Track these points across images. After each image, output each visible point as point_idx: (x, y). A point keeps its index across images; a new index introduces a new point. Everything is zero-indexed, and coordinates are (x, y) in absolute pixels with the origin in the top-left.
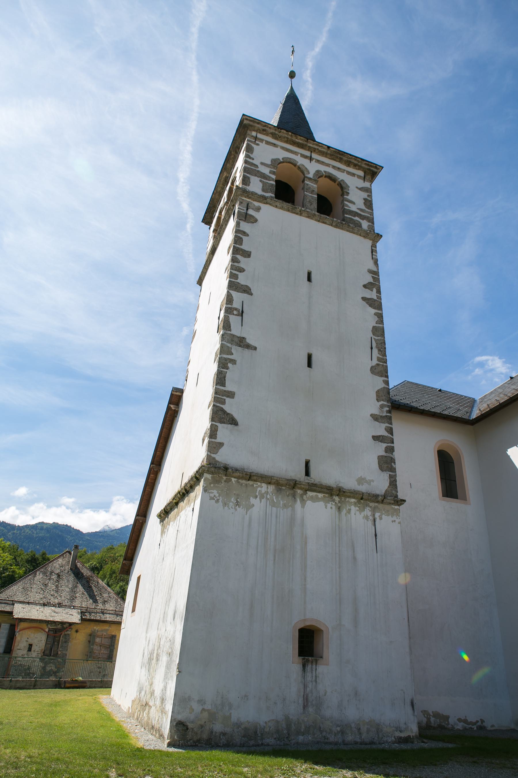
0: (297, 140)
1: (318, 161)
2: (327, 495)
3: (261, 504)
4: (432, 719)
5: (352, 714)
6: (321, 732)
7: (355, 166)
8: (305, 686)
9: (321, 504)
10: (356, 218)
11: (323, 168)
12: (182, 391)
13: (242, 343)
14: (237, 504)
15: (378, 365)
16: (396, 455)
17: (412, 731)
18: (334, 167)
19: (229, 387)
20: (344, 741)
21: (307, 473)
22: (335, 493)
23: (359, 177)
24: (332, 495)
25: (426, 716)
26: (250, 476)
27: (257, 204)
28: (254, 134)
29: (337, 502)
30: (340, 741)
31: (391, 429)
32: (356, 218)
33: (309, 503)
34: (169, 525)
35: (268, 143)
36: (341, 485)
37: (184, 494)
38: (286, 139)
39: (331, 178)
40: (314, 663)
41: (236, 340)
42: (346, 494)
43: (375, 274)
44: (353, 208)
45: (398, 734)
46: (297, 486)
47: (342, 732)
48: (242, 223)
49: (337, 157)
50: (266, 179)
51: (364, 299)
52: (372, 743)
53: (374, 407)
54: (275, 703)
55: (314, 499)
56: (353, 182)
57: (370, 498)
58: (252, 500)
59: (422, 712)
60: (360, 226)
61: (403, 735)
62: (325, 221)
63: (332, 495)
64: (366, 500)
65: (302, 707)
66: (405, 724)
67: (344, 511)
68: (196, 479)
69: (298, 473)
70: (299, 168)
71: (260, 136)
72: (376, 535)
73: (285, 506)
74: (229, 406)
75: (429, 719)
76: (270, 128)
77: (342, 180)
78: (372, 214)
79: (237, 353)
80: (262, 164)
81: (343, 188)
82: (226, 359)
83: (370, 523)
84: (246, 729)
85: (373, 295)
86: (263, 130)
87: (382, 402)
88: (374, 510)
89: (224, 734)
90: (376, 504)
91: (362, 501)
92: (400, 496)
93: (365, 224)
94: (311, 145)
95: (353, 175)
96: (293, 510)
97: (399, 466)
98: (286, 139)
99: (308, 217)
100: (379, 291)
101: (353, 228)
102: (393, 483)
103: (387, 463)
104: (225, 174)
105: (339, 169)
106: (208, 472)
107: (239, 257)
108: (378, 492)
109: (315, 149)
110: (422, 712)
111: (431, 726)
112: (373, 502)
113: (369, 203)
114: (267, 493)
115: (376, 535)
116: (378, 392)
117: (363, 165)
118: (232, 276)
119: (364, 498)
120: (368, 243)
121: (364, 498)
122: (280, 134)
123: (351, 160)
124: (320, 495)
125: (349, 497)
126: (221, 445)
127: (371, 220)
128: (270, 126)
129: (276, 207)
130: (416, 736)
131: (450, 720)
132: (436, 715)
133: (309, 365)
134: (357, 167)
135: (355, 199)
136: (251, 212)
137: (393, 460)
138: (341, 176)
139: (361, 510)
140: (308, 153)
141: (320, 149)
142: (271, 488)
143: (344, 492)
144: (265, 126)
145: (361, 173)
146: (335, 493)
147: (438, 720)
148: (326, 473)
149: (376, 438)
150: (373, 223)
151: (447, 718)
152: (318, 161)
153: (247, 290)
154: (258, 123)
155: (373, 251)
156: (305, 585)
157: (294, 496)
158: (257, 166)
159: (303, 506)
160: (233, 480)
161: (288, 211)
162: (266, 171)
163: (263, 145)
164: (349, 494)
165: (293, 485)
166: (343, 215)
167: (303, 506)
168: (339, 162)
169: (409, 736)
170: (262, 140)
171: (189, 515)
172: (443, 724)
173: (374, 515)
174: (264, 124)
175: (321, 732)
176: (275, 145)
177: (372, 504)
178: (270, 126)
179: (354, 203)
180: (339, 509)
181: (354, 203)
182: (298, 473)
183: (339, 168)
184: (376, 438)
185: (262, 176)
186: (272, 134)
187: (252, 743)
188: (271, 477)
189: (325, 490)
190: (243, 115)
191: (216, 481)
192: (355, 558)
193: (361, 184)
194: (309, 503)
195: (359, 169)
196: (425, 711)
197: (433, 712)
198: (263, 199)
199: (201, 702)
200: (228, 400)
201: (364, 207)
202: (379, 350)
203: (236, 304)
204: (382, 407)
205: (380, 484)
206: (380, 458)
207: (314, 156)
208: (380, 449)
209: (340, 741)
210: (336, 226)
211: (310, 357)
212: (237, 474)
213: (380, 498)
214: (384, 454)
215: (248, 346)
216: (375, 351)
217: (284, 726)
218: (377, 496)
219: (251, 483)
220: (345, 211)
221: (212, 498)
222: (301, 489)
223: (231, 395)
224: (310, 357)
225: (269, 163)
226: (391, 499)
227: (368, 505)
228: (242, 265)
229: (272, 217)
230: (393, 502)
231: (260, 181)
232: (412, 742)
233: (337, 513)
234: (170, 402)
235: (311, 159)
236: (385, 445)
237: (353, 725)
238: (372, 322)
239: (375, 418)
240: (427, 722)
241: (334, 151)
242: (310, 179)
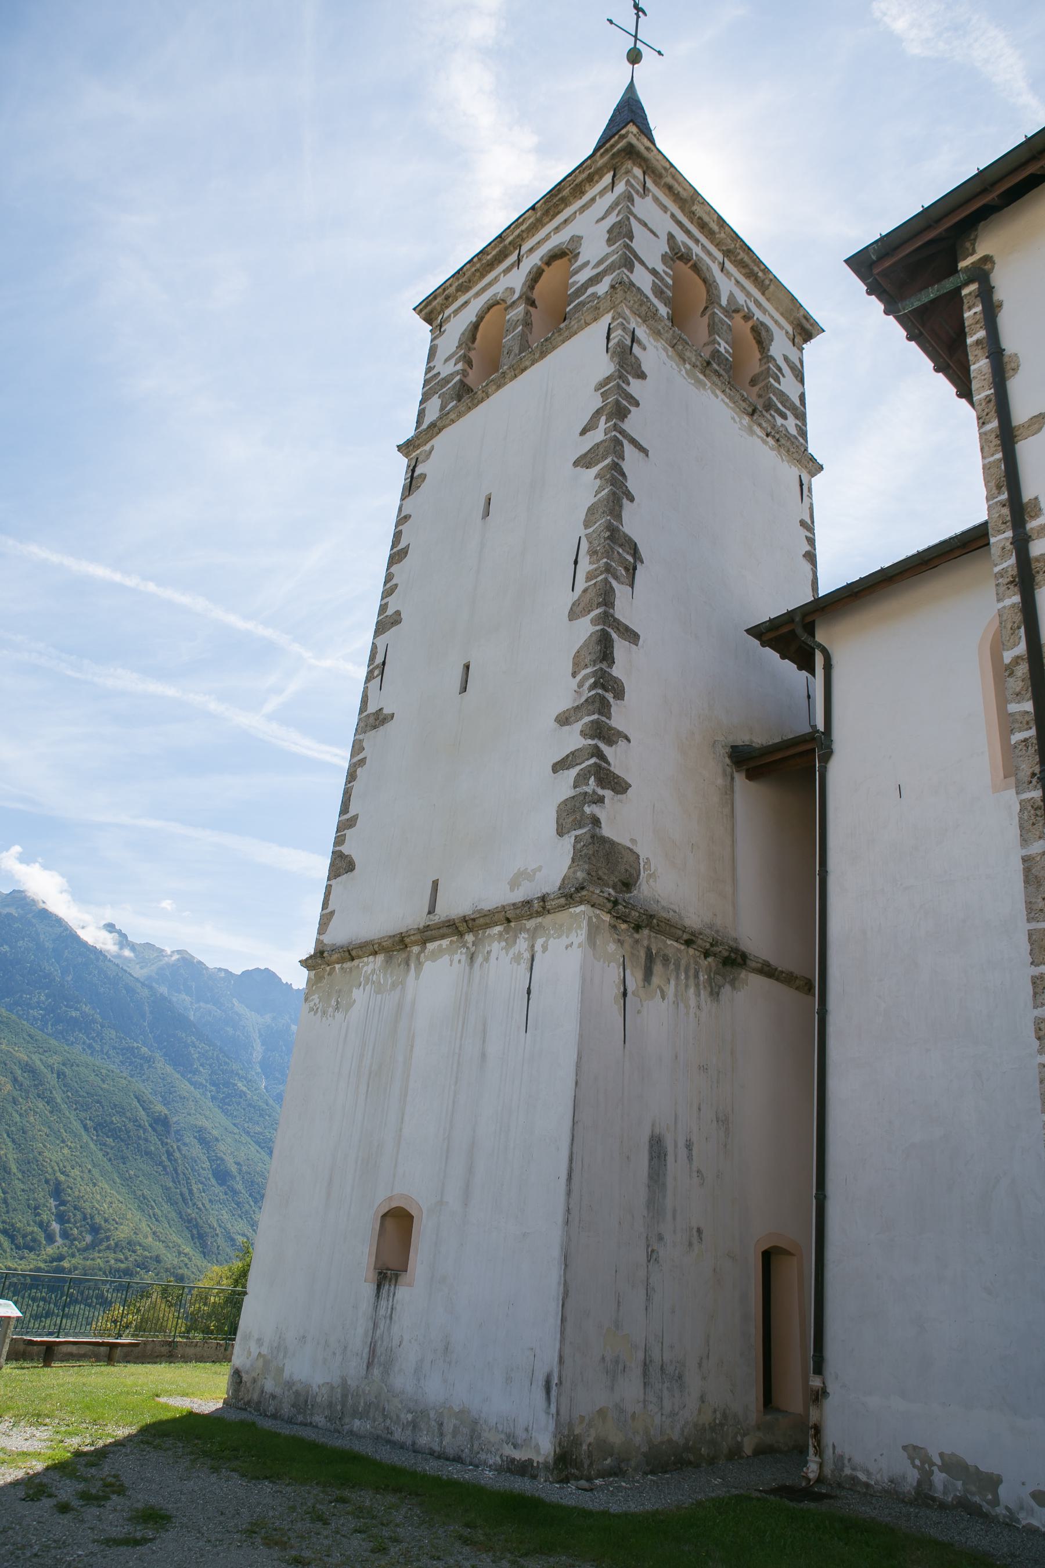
0: (489, 257)
2: (455, 938)
4: (939, 1478)
5: (434, 1391)
6: (385, 1417)
7: (591, 179)
8: (375, 1326)
17: (537, 1448)
20: (414, 1444)
24: (461, 935)
25: (917, 1462)
29: (470, 945)
30: (409, 1442)
38: (478, 274)
40: (393, 1282)
42: (477, 922)
45: (509, 1451)
47: (414, 1425)
49: (556, 205)
50: (448, 382)
52: (458, 1459)
54: (334, 1354)
57: (518, 911)
59: (905, 1448)
61: (519, 1455)
62: (522, 366)
63: (461, 935)
64: (519, 918)
65: (365, 1367)
66: (527, 1430)
67: (479, 959)
72: (529, 992)
75: (926, 1477)
76: (451, 285)
83: (524, 966)
84: (297, 1394)
86: (447, 298)
89: (273, 1397)
90: (539, 919)
91: (512, 924)
94: (511, 238)
98: (478, 274)
99: (499, 387)
101: (567, 328)
109: (519, 236)
110: (905, 1448)
111: (934, 1499)
112: (530, 917)
115: (529, 992)
117: (601, 163)
123: (578, 181)
124: (445, 943)
125: (488, 926)
128: (448, 284)
129: (453, 421)
130: (546, 1466)
131: (1002, 1490)
132: (953, 1466)
134: (596, 178)
141: (523, 227)
142: (380, 958)
143: (474, 920)
144: (444, 290)
147: (959, 1484)
151: (993, 1482)
154: (435, 298)
156: (401, 1129)
159: (417, 978)
161: (470, 409)
164: (481, 921)
168: (566, 206)
169: (530, 1461)
172: (977, 1499)
173: (533, 946)
174: (440, 290)
175: (385, 1417)
177: (530, 924)
178: (448, 284)
183: (566, 221)
186: (458, 290)
187: (300, 1418)
189: (445, 930)
190: (414, 309)
192: (483, 1056)
195: (601, 178)
196: (915, 1448)
197: (941, 1455)
199: (260, 1342)
209: (409, 1442)
212: (335, 957)
213: (536, 905)
217: (339, 1396)
222: (415, 943)
227: (523, 929)
230: (563, 901)
232: (534, 1477)
233: (467, 968)
237: (432, 1414)
240: (919, 1483)
241: (545, 203)
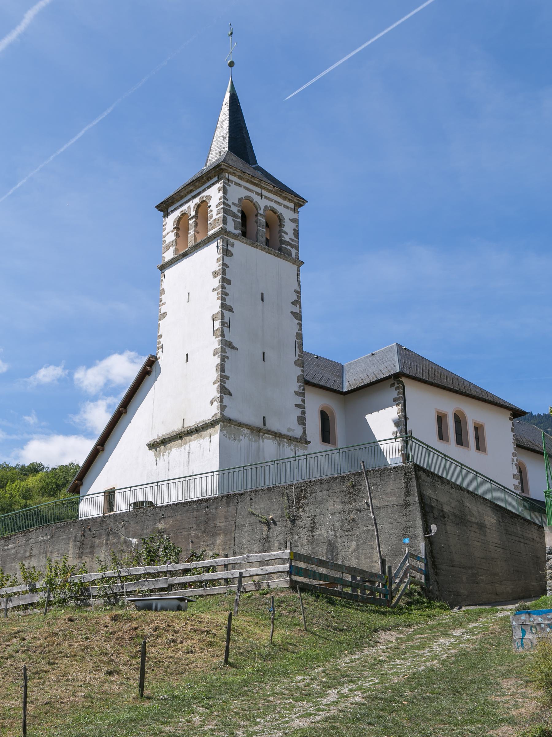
1: (266, 197)
3: (245, 439)
9: (271, 441)
10: (289, 247)
14: (235, 439)
15: (298, 359)
16: (307, 416)
18: (276, 202)
19: (227, 373)
21: (264, 424)
22: (277, 435)
23: (291, 209)
24: (276, 436)
26: (240, 424)
27: (232, 240)
28: (227, 175)
31: (304, 400)
32: (289, 247)
33: (265, 440)
34: (171, 450)
35: (236, 184)
36: (280, 431)
39: (274, 211)
41: (228, 343)
43: (298, 292)
46: (260, 431)
48: (225, 257)
51: (292, 313)
53: (295, 386)
55: (268, 438)
56: (287, 214)
58: (241, 437)
60: (290, 255)
63: (276, 436)
64: (293, 440)
67: (281, 446)
68: (211, 424)
70: (254, 204)
71: (232, 178)
73: (255, 441)
77: (281, 214)
78: (298, 243)
79: (229, 352)
80: (233, 203)
81: (280, 219)
82: (224, 356)
85: (296, 309)
86: (233, 173)
87: (300, 384)
88: (295, 446)
92: (308, 439)
93: (293, 251)
96: (259, 443)
97: (307, 422)
99: (261, 249)
100: (300, 307)
101: (287, 258)
102: (304, 432)
103: (302, 420)
104: (192, 188)
106: (222, 421)
107: (225, 284)
108: (297, 437)
113: (296, 233)
114: (247, 433)
116: (298, 377)
117: (295, 200)
118: (223, 299)
119: (291, 439)
120: (296, 267)
121: (291, 439)
122: (244, 176)
124: (271, 436)
125: (284, 438)
126: (225, 406)
127: (297, 248)
133: (264, 360)
136: (230, 248)
137: (305, 419)
138: (280, 209)
139: (289, 446)
140: (259, 190)
141: (268, 187)
142: (249, 431)
145: (292, 205)
148: (274, 425)
149: (297, 405)
150: (298, 251)
152: (266, 197)
153: (230, 309)
157: (259, 436)
158: (229, 206)
159: (263, 442)
160: (232, 426)
161: (250, 245)
162: (235, 209)
165: (259, 430)
166: (281, 244)
167: (263, 442)
176: (240, 185)
177: (294, 443)
179: (287, 234)
181: (287, 234)
182: (260, 424)
184: (297, 405)
185: (234, 215)
188: (249, 426)
193: (293, 216)
194: (265, 440)
198: (235, 237)
200: (227, 381)
201: (293, 237)
202: (300, 349)
203: (226, 320)
204: (300, 386)
205: (298, 433)
206: (298, 417)
207: (265, 193)
208: (298, 412)
210: (277, 256)
211: (264, 353)
212: (235, 423)
213: (299, 440)
214: (300, 415)
215: (234, 348)
218: (297, 439)
219: (240, 428)
220: (282, 242)
221: (224, 435)
222: (262, 432)
223: (228, 378)
224: (264, 353)
226: (303, 441)
227: (292, 443)
228: (227, 291)
229: (240, 248)
231: (233, 220)
235: (262, 195)
236: (301, 410)
238: (296, 330)
239: (297, 393)
242: (261, 215)
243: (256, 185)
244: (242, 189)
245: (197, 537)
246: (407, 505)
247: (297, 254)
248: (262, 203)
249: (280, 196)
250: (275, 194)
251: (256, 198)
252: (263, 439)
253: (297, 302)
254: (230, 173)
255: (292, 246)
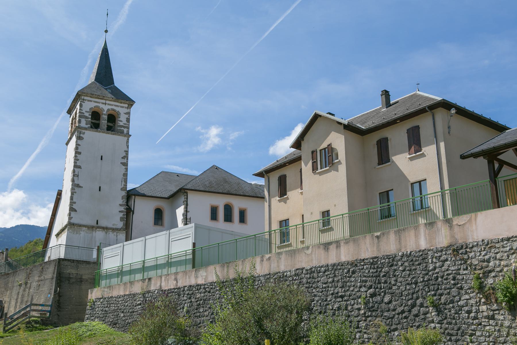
1: (109, 104)
3: (83, 233)
10: (122, 128)
11: (110, 107)
12: (61, 191)
13: (78, 186)
18: (115, 105)
19: (74, 200)
21: (97, 224)
22: (105, 229)
23: (125, 108)
26: (80, 226)
27: (83, 131)
33: (97, 232)
35: (88, 101)
37: (62, 230)
43: (127, 152)
44: (121, 124)
48: (78, 141)
51: (121, 163)
69: (94, 224)
71: (86, 98)
74: (74, 206)
79: (77, 189)
80: (86, 112)
85: (125, 161)
88: (117, 233)
93: (125, 130)
95: (123, 107)
100: (127, 159)
105: (117, 106)
113: (128, 120)
118: (75, 162)
135: (123, 118)
136: (81, 135)
140: (104, 101)
142: (86, 228)
145: (126, 105)
146: (105, 229)
148: (103, 223)
152: (109, 104)
153: (79, 167)
155: (128, 142)
162: (87, 114)
163: (86, 102)
165: (93, 227)
170: (86, 100)
171: (63, 238)
176: (91, 101)
179: (121, 121)
180: (106, 233)
181: (121, 121)
182: (94, 224)
185: (86, 117)
191: (71, 228)
193: (126, 111)
194: (97, 232)
198: (86, 129)
201: (126, 122)
203: (76, 173)
207: (107, 102)
211: (100, 187)
215: (80, 187)
216: (123, 182)
224: (100, 187)
225: (89, 110)
228: (78, 158)
234: (57, 195)
235: (105, 104)
238: (123, 171)
239: (121, 205)
243: (102, 99)
244: (93, 102)
245: (3, 292)
246: (53, 278)
247: (128, 132)
248: (106, 108)
249: (118, 102)
250: (114, 101)
251: (101, 106)
252: (95, 232)
253: (126, 157)
254: (84, 96)
255: (124, 127)
